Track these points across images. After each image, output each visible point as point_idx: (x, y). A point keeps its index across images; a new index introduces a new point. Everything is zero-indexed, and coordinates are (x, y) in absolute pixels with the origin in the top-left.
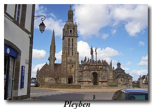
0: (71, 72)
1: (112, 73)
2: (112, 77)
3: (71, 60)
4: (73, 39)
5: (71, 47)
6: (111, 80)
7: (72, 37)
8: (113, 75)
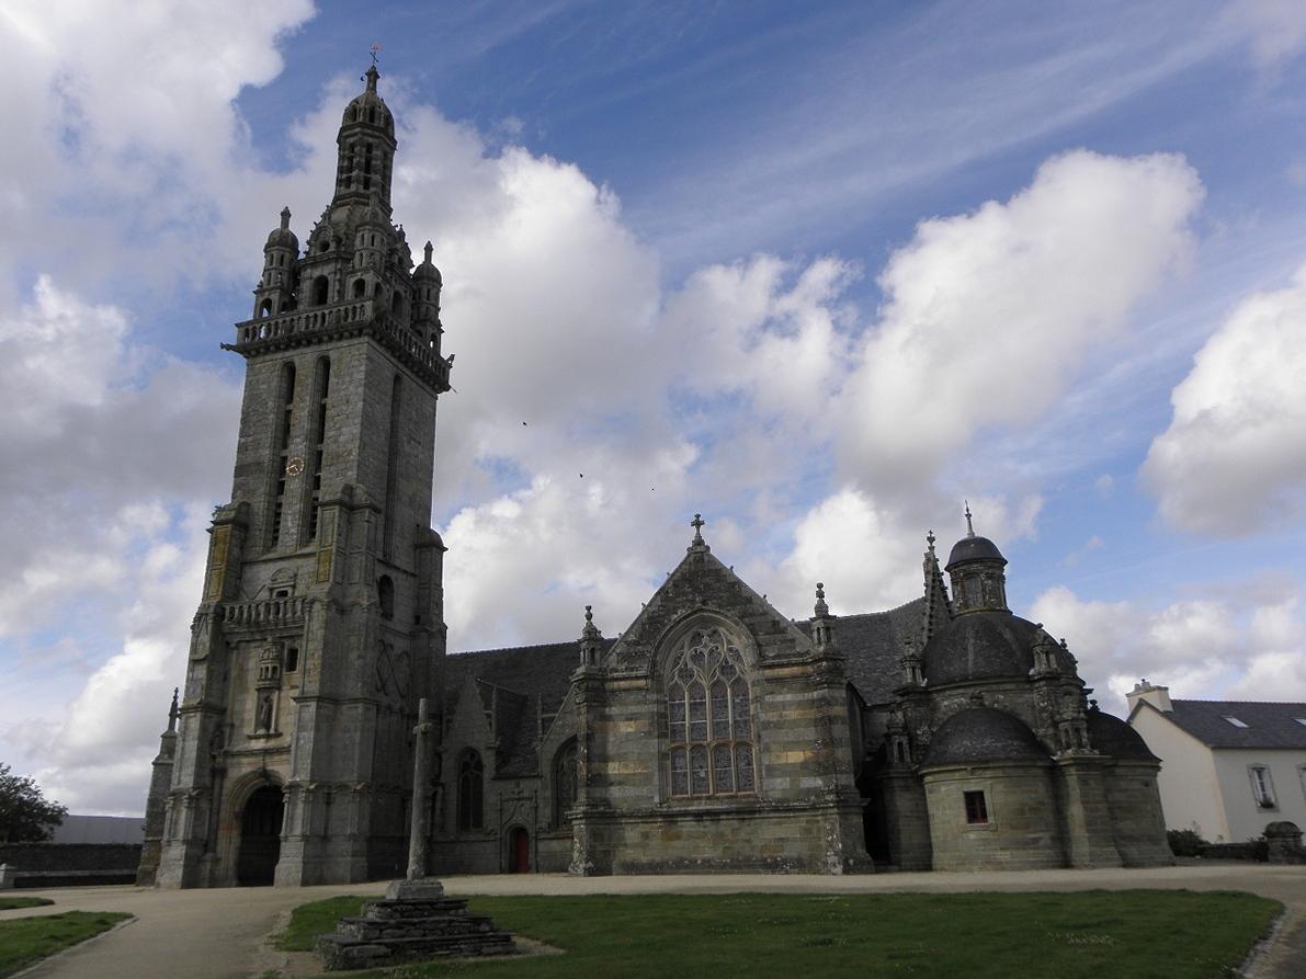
0: (268, 737)
1: (800, 704)
2: (796, 757)
3: (284, 594)
4: (325, 363)
5: (298, 448)
6: (783, 808)
7: (307, 340)
8: (816, 722)
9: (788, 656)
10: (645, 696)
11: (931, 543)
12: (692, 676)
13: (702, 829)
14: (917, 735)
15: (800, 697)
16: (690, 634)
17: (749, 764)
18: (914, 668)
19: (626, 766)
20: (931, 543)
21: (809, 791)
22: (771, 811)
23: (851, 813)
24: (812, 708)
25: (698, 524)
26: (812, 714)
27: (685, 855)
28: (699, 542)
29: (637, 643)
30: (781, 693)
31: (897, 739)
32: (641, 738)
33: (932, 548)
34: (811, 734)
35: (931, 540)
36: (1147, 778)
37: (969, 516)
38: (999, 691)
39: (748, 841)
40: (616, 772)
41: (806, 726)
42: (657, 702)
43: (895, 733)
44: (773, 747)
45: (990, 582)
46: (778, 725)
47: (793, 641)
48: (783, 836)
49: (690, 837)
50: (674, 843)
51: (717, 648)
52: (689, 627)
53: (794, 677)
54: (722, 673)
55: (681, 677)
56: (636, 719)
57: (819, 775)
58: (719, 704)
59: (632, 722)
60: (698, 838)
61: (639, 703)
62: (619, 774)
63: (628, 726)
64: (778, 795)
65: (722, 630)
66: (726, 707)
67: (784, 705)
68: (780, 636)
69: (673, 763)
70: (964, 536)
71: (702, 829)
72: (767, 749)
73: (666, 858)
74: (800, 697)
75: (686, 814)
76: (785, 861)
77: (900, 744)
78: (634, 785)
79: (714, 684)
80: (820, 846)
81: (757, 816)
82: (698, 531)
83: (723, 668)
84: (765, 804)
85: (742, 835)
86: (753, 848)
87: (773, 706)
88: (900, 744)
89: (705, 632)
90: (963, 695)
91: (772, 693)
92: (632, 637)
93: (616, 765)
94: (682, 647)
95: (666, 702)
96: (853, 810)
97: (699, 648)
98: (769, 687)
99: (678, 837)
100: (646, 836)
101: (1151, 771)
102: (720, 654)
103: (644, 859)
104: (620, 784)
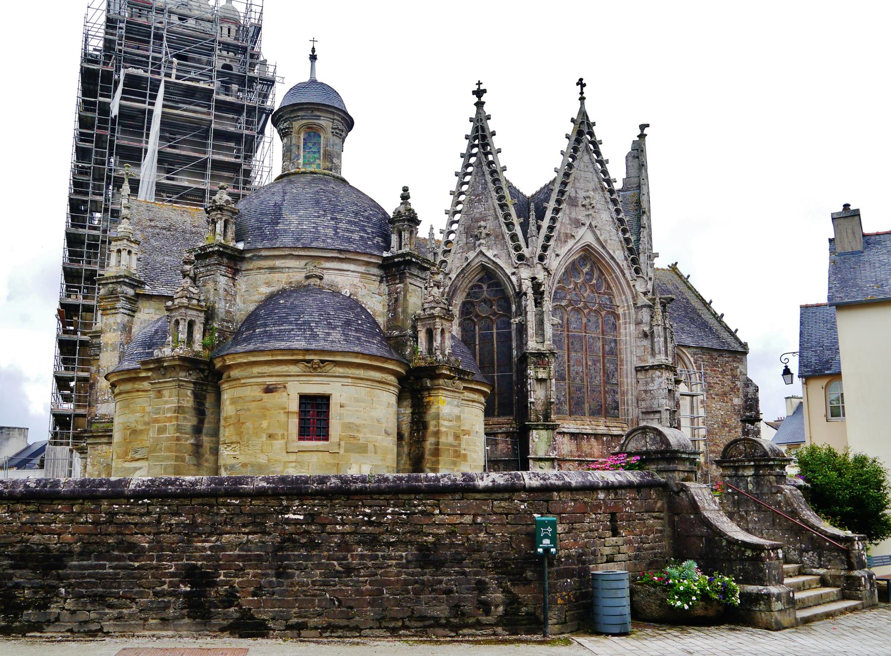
23: (101, 444)
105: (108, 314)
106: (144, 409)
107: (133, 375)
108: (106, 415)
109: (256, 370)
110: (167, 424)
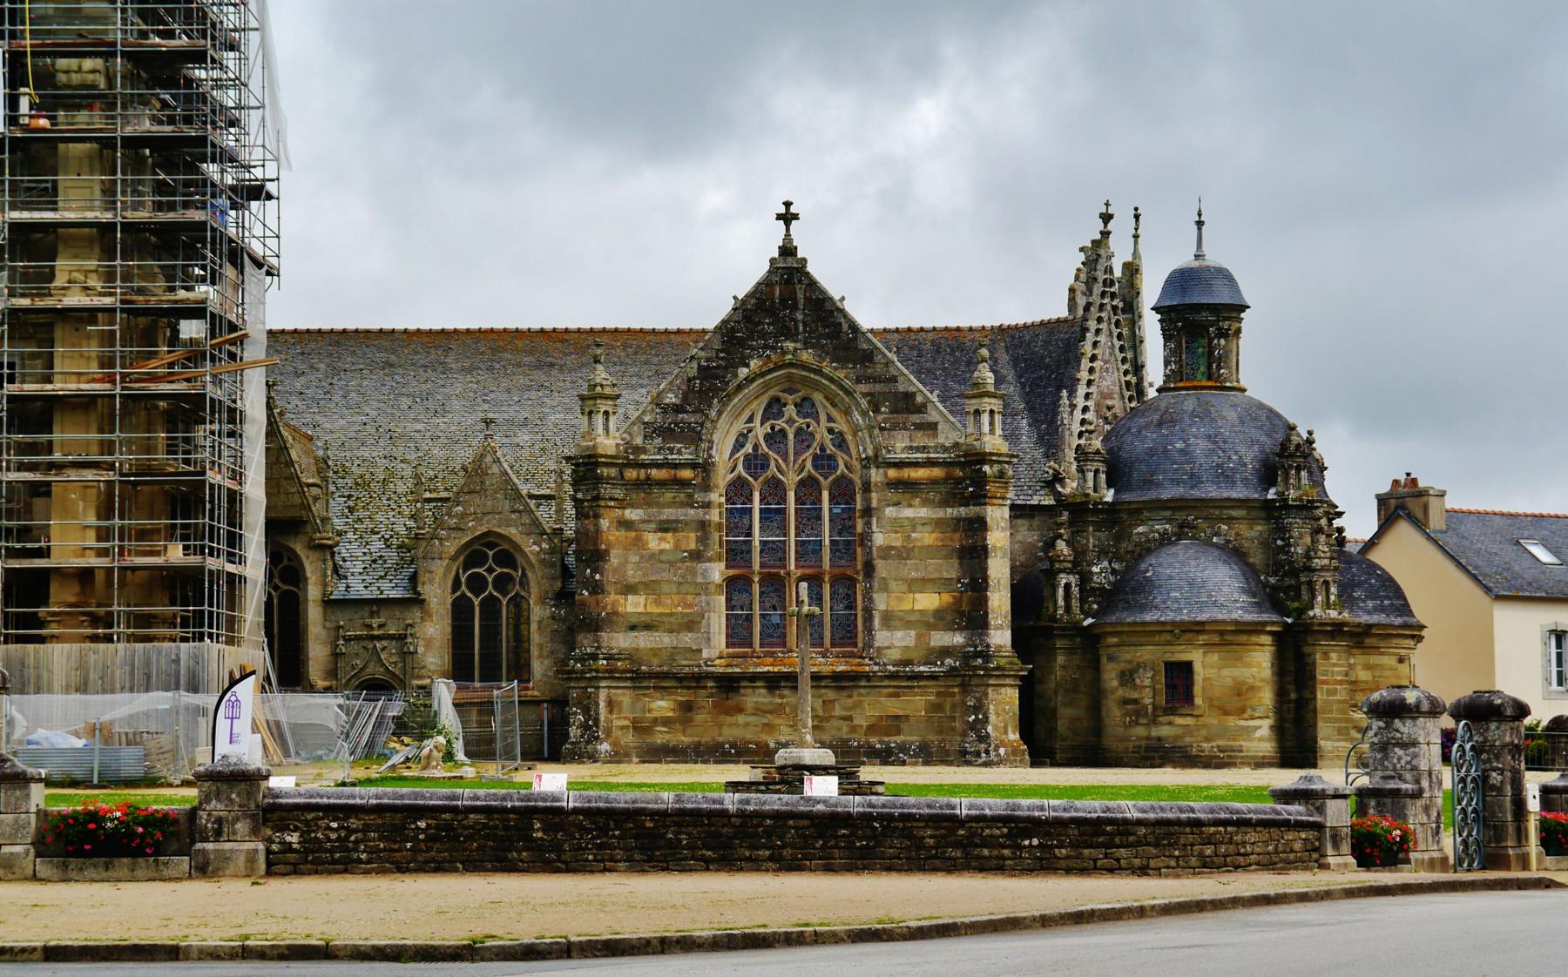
2: (929, 601)
6: (903, 677)
9: (924, 449)
10: (690, 496)
11: (1106, 224)
12: (765, 466)
13: (779, 701)
14: (1091, 573)
15: (940, 513)
16: (765, 400)
17: (851, 606)
18: (1097, 472)
19: (658, 602)
20: (1106, 224)
21: (945, 652)
22: (887, 677)
23: (1004, 685)
24: (955, 531)
25: (787, 218)
26: (957, 540)
27: (749, 736)
28: (787, 250)
29: (678, 409)
30: (910, 506)
31: (1063, 579)
32: (683, 560)
33: (1106, 234)
34: (951, 570)
35: (1106, 218)
36: (1403, 652)
37: (1200, 224)
38: (1221, 520)
39: (849, 718)
40: (641, 610)
41: (946, 557)
42: (707, 505)
43: (1063, 571)
44: (893, 585)
45: (1222, 342)
46: (904, 554)
47: (932, 427)
48: (901, 713)
49: (759, 711)
50: (729, 719)
51: (808, 426)
52: (767, 387)
53: (934, 482)
54: (815, 467)
55: (747, 467)
56: (675, 530)
57: (961, 629)
58: (810, 517)
59: (669, 536)
60: (770, 712)
61: (682, 505)
62: (646, 614)
63: (661, 539)
64: (895, 655)
65: (818, 397)
66: (819, 518)
67: (914, 524)
68: (916, 418)
69: (728, 600)
70: (1184, 258)
71: (779, 701)
72: (885, 588)
73: (721, 739)
74: (940, 513)
75: (754, 678)
76: (903, 748)
77: (1067, 586)
78: (671, 631)
79: (802, 483)
80: (953, 729)
81: (863, 683)
82: (788, 229)
83: (816, 458)
84: (876, 668)
85: (838, 711)
86: (853, 729)
87: (897, 525)
88: (1067, 586)
89: (790, 398)
90: (1169, 521)
91: (897, 504)
92: (671, 398)
93: (641, 599)
94: (750, 420)
95: (720, 505)
96: (1008, 681)
97: (780, 423)
98: (891, 495)
99: (740, 710)
100: (687, 707)
101: (1411, 643)
102: (812, 434)
103: (685, 740)
104: (648, 627)
105: (995, 505)
106: (1260, 664)
107: (1259, 628)
108: (1001, 646)
109: (1395, 641)
110: (1338, 687)
